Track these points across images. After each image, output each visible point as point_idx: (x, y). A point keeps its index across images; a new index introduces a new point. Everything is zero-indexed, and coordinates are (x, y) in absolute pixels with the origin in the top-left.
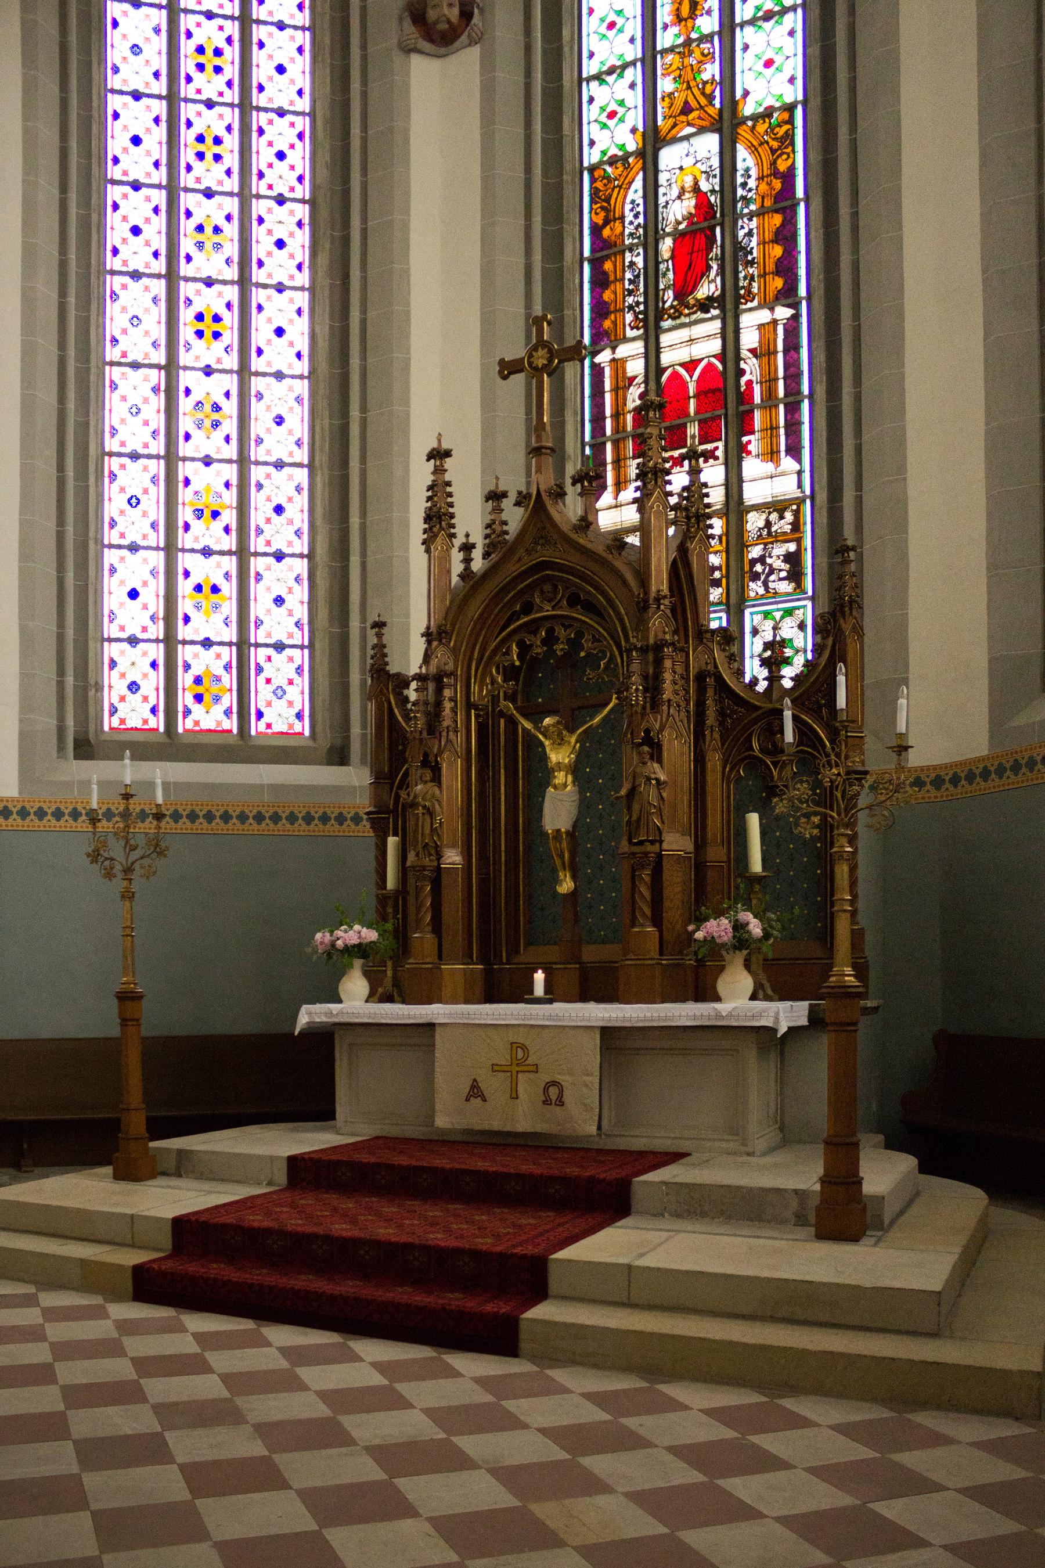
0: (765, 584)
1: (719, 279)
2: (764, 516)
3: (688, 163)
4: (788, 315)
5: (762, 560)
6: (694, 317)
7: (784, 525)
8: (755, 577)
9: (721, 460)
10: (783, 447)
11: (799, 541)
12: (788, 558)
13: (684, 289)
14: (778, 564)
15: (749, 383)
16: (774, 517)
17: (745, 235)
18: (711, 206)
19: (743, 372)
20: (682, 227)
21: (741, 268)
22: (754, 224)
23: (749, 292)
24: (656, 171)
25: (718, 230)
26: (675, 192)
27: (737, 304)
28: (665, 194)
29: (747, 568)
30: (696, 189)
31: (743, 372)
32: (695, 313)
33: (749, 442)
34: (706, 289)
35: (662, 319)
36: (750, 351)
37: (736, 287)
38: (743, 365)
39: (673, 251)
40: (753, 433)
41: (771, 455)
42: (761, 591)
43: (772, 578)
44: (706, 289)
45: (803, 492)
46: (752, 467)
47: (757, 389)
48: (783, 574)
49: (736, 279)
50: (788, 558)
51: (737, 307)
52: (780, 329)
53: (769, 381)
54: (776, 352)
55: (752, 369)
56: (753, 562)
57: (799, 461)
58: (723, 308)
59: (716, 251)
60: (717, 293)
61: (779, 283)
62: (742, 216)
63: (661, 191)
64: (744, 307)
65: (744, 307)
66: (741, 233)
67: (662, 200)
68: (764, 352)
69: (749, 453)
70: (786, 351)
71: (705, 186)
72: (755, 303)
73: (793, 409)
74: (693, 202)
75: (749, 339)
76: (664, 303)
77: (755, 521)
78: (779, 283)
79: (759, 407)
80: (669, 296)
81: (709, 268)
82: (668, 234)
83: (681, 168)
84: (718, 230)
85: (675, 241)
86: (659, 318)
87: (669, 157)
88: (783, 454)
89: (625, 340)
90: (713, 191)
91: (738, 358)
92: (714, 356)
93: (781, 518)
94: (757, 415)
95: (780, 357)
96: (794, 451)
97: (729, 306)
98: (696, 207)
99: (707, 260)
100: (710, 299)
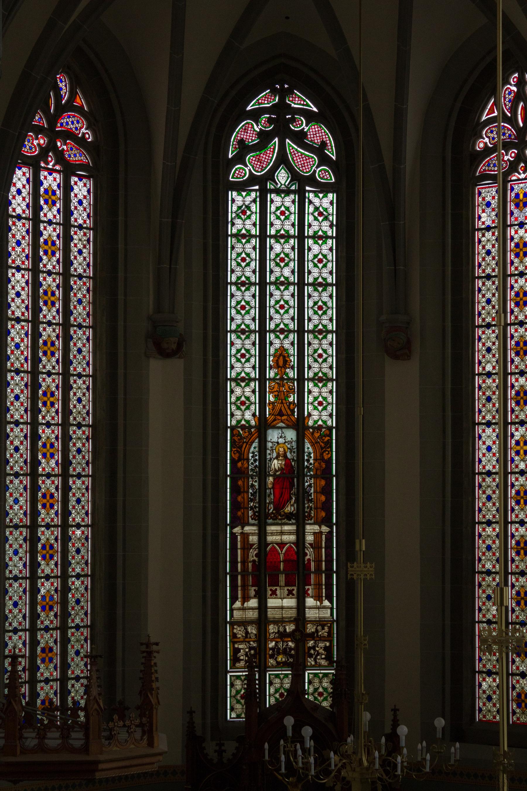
0: (315, 660)
1: (295, 505)
2: (315, 627)
3: (281, 441)
4: (327, 531)
5: (314, 648)
6: (283, 521)
7: (324, 633)
8: (311, 656)
9: (295, 596)
10: (324, 595)
11: (331, 642)
12: (325, 648)
13: (279, 506)
14: (321, 651)
15: (309, 560)
16: (319, 628)
17: (308, 486)
18: (292, 467)
19: (306, 554)
20: (278, 473)
21: (306, 502)
22: (312, 481)
23: (310, 513)
24: (266, 441)
25: (295, 480)
26: (275, 455)
27: (304, 520)
28: (270, 454)
29: (306, 651)
30: (285, 456)
31: (306, 554)
32: (284, 519)
33: (309, 589)
34: (289, 509)
35: (267, 518)
36: (309, 544)
37: (304, 512)
38: (307, 551)
39: (274, 484)
40: (311, 585)
41: (318, 597)
42: (313, 663)
43: (319, 657)
44: (289, 509)
45: (333, 618)
46: (310, 602)
47: (312, 564)
48: (323, 656)
49: (304, 507)
50: (325, 648)
51: (304, 522)
52: (324, 536)
53: (318, 561)
54: (321, 548)
55: (310, 553)
56: (310, 648)
57: (331, 602)
58: (297, 519)
59: (294, 491)
60: (294, 512)
62: (307, 476)
63: (268, 452)
64: (307, 522)
65: (307, 522)
66: (306, 484)
67: (268, 457)
68: (316, 546)
69: (309, 595)
70: (326, 548)
71: (289, 455)
72: (312, 521)
73: (329, 578)
74: (284, 463)
75: (310, 538)
76: (269, 510)
77: (310, 628)
79: (313, 572)
80: (271, 508)
81: (291, 498)
82: (271, 475)
83: (278, 443)
84: (295, 480)
85: (274, 480)
86: (266, 518)
87: (273, 436)
88: (324, 598)
90: (293, 460)
91: (304, 547)
92: (293, 543)
93: (323, 629)
94: (312, 576)
95: (323, 550)
96: (329, 598)
97: (300, 520)
98: (285, 465)
99: (290, 494)
100: (291, 514)
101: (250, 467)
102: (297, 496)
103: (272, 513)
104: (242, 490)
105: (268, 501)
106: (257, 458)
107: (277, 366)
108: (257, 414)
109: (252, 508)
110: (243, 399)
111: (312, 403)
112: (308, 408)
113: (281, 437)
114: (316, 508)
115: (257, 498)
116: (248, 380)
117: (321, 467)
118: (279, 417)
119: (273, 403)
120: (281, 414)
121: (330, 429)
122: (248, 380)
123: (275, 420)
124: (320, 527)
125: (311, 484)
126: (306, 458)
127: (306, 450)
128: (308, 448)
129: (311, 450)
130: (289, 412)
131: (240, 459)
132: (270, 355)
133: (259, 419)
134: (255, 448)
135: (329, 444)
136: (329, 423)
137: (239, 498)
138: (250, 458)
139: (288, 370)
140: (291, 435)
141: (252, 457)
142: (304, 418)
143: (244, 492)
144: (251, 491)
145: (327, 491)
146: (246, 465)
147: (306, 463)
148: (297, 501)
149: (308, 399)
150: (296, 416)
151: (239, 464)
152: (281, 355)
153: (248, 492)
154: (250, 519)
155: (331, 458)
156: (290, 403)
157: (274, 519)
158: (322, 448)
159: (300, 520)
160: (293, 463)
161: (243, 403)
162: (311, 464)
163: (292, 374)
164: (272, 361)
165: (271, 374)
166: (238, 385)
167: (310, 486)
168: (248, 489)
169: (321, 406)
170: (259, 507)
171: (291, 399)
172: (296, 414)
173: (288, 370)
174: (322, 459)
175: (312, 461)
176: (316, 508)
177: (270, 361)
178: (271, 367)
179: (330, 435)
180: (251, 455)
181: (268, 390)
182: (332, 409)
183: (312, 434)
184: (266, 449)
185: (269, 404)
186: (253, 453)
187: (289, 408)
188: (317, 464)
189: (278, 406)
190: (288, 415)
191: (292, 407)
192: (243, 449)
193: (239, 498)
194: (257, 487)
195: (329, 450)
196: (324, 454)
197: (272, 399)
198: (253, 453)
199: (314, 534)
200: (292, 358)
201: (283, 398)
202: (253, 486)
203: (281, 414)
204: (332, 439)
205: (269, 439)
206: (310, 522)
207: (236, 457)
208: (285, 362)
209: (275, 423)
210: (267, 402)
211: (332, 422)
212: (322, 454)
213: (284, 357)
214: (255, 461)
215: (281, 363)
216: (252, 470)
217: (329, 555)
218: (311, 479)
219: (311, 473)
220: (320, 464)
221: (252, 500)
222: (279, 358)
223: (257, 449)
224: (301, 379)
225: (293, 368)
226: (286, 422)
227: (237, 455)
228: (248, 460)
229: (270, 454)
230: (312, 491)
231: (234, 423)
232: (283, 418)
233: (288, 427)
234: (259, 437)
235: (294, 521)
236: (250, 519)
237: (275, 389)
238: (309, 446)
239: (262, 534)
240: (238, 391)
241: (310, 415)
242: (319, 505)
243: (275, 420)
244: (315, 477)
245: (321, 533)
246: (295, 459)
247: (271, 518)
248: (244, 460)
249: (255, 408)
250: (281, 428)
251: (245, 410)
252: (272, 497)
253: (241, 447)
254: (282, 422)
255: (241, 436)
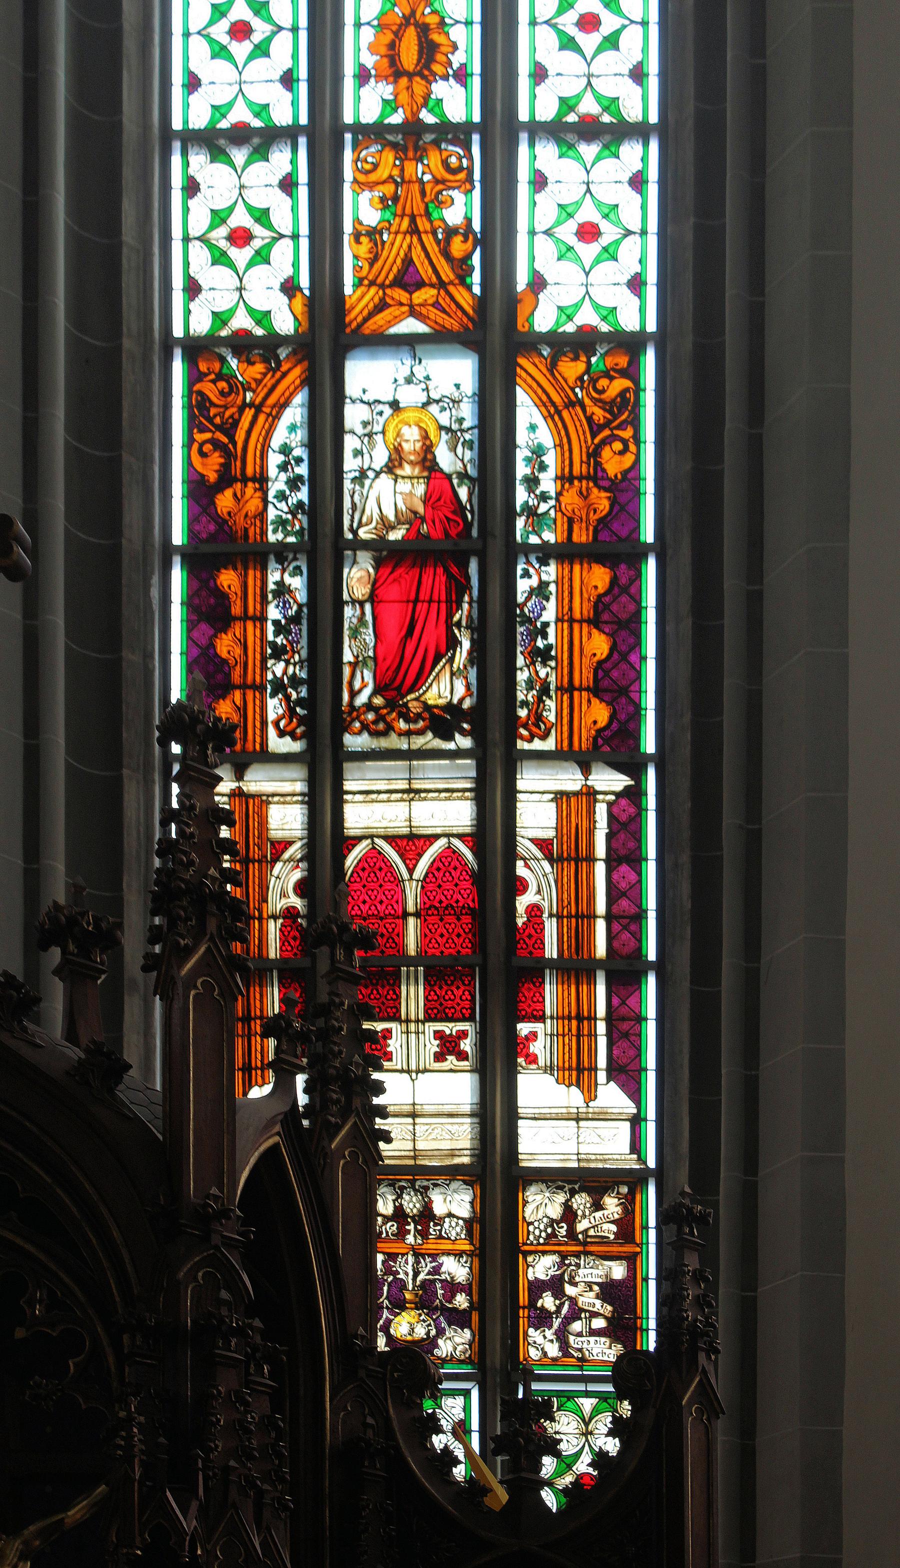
1: (473, 674)
19: (521, 886)
20: (396, 535)
27: (512, 737)
28: (358, 453)
31: (521, 886)
44: (446, 688)
47: (551, 928)
53: (577, 917)
61: (600, 713)
66: (523, 586)
68: (566, 852)
70: (612, 862)
71: (445, 460)
74: (420, 489)
75: (535, 817)
78: (600, 713)
83: (395, 405)
84: (473, 568)
89: (266, 757)
91: (511, 854)
95: (600, 869)
97: (494, 741)
99: (449, 625)
101: (272, 513)
102: (479, 630)
103: (369, 706)
104: (236, 609)
105: (348, 656)
106: (303, 470)
107: (394, 71)
108: (304, 282)
109: (279, 687)
110: (240, 219)
111: (548, 233)
112: (533, 255)
113: (409, 381)
114: (568, 689)
115: (304, 642)
116: (262, 139)
117: (591, 508)
118: (400, 294)
119: (373, 233)
120: (407, 279)
121: (630, 344)
122: (262, 139)
123: (381, 306)
124: (586, 771)
125: (543, 585)
126: (522, 470)
127: (522, 436)
128: (533, 428)
129: (545, 436)
130: (447, 272)
131: (226, 479)
132: (358, 25)
133: (311, 304)
134: (293, 428)
135: (625, 408)
136: (629, 321)
137: (225, 645)
138: (272, 471)
139: (439, 89)
140: (455, 373)
141: (283, 467)
142: (512, 301)
143: (245, 617)
144: (274, 613)
145: (614, 614)
146: (253, 505)
147: (521, 495)
148: (478, 656)
149: (533, 212)
150: (477, 290)
151: (225, 501)
152: (408, 20)
153: (262, 618)
154: (272, 732)
155: (633, 474)
156: (451, 232)
157: (375, 734)
158: (595, 428)
159: (494, 741)
160: (463, 493)
161: (240, 237)
162: (544, 497)
163: (457, 102)
164: (372, 49)
165: (365, 103)
166: (217, 154)
167: (541, 590)
168: (264, 602)
169: (593, 248)
170: (312, 682)
171: (453, 216)
172: (476, 277)
173: (439, 89)
174: (597, 476)
175: (548, 483)
176: (568, 689)
177: (359, 47)
178: (363, 76)
179: (632, 372)
180: (274, 459)
181: (348, 174)
182: (642, 254)
183: (552, 366)
184: (339, 430)
185: (357, 236)
186: (285, 450)
187: (446, 254)
188: (571, 498)
189: (396, 247)
190: (442, 285)
191: (458, 247)
192: (240, 436)
193: (225, 645)
194: (302, 596)
195: (627, 434)
196: (606, 453)
197: (371, 217)
198: (285, 450)
199: (560, 797)
200: (457, 34)
201: (418, 208)
202: (282, 590)
203: (407, 279)
204: (638, 389)
205: (352, 388)
206: (537, 745)
207: (210, 469)
208: (429, 51)
209: (380, 319)
210: (348, 227)
211: (638, 314)
212: (594, 454)
213: (424, 30)
214: (294, 483)
215: (409, 56)
216: (281, 523)
217: (624, 894)
218: (544, 562)
219: (549, 537)
220: (584, 496)
221: (278, 653)
222: (398, 35)
223: (300, 435)
224: (500, 127)
225: (462, 76)
226: (433, 313)
227: (216, 459)
228: (262, 480)
229: (358, 453)
230: (549, 615)
231: (201, 325)
232: (419, 297)
233: (440, 338)
234: (310, 381)
235: (465, 743)
236: (272, 732)
237: (383, 172)
238: (538, 418)
239: (324, 802)
240: (216, 179)
241: (538, 283)
242: (584, 675)
243: (381, 306)
244: (564, 553)
245: (591, 794)
246: (472, 471)
247: (365, 727)
248: (245, 480)
249: (290, 259)
250: (410, 342)
251: (250, 265)
252: (369, 636)
253: (230, 429)
254: (413, 312)
255: (230, 379)
